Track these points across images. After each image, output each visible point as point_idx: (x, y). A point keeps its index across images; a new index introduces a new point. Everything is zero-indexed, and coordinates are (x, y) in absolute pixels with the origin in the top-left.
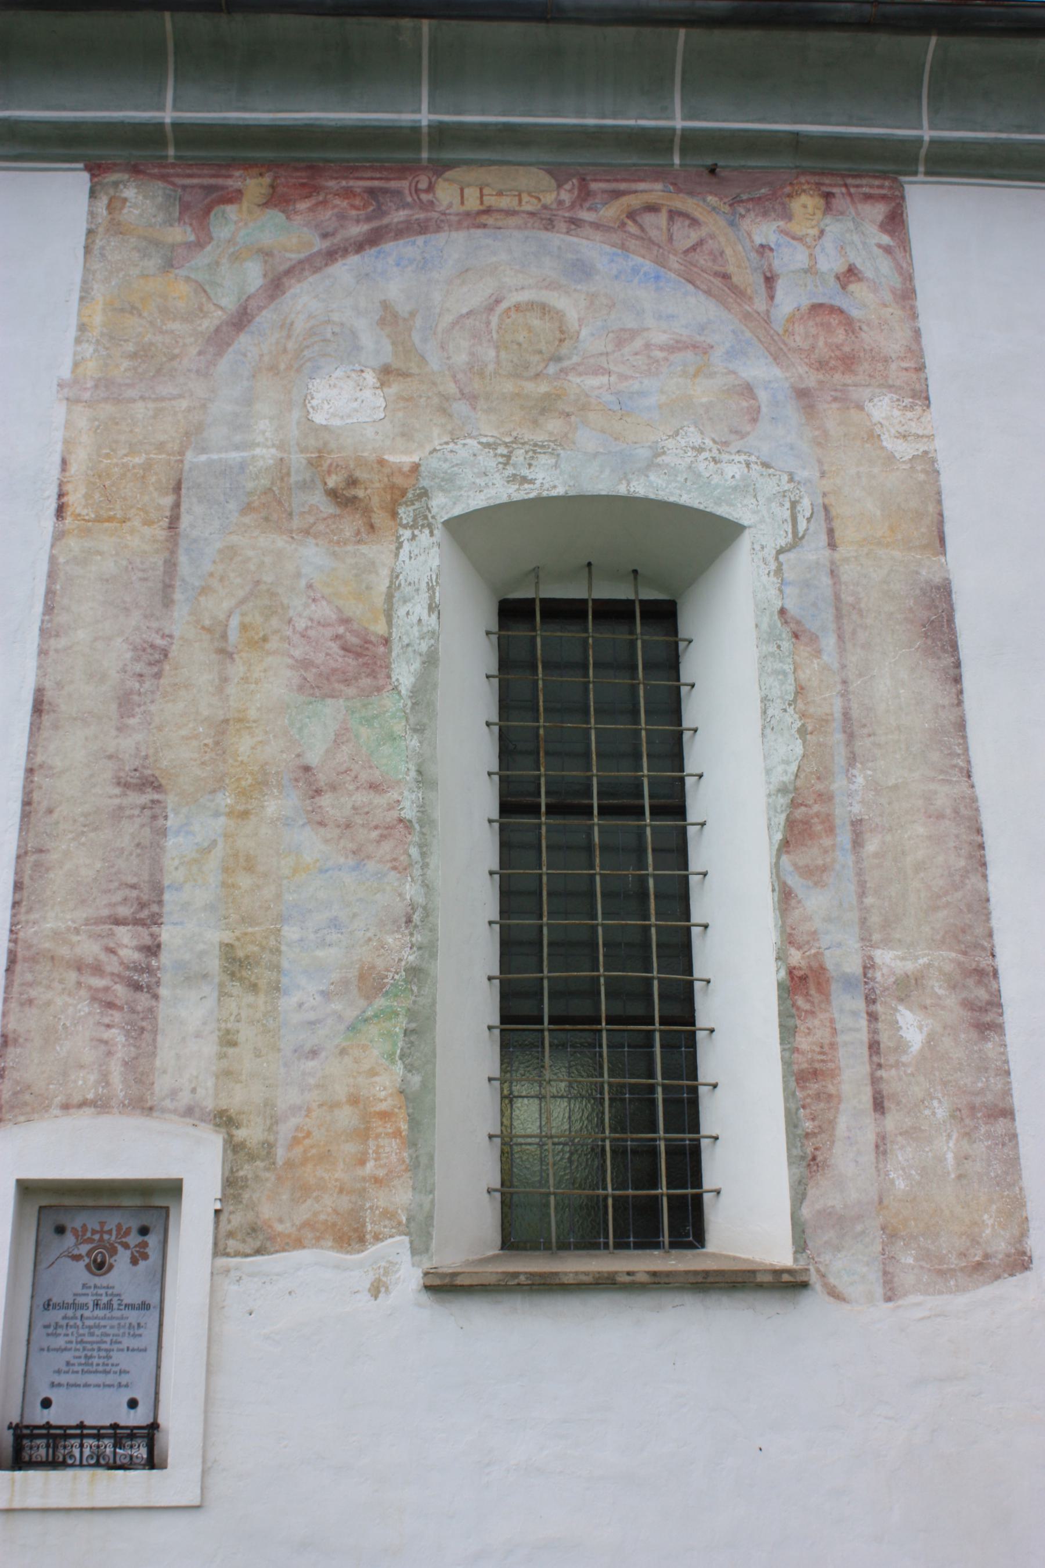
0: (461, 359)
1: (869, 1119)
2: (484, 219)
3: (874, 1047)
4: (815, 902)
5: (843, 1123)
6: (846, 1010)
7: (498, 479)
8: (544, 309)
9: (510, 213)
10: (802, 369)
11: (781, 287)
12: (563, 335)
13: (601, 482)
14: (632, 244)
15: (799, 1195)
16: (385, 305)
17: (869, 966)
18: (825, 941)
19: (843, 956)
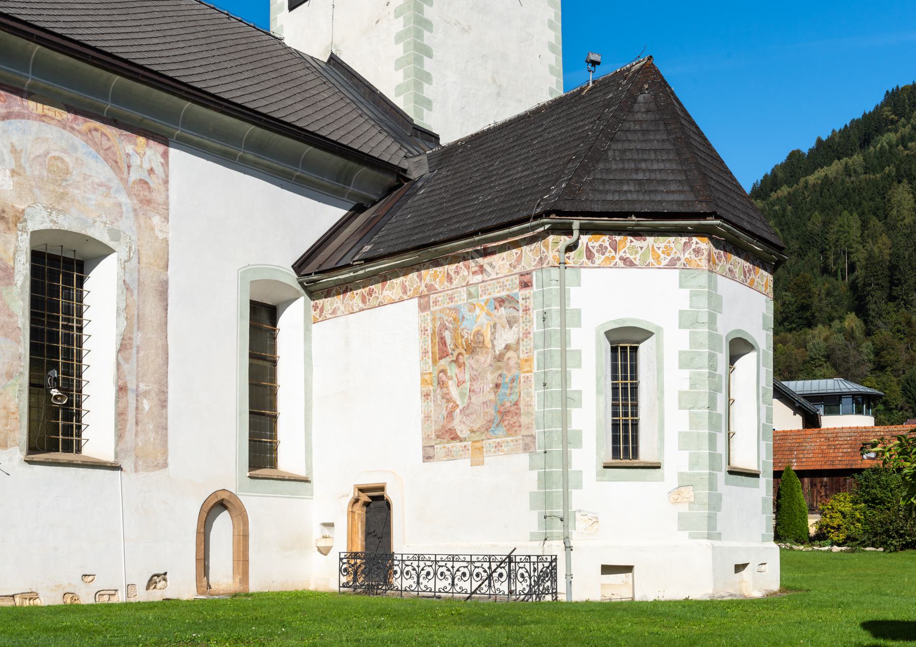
0: (37, 173)
1: (134, 426)
2: (43, 118)
3: (137, 408)
4: (125, 367)
5: (128, 426)
6: (131, 397)
7: (47, 220)
8: (62, 160)
9: (52, 119)
10: (135, 201)
11: (132, 169)
12: (67, 172)
13: (76, 228)
14: (90, 142)
15: (117, 445)
16: (12, 145)
17: (138, 386)
18: (128, 378)
19: (131, 386)
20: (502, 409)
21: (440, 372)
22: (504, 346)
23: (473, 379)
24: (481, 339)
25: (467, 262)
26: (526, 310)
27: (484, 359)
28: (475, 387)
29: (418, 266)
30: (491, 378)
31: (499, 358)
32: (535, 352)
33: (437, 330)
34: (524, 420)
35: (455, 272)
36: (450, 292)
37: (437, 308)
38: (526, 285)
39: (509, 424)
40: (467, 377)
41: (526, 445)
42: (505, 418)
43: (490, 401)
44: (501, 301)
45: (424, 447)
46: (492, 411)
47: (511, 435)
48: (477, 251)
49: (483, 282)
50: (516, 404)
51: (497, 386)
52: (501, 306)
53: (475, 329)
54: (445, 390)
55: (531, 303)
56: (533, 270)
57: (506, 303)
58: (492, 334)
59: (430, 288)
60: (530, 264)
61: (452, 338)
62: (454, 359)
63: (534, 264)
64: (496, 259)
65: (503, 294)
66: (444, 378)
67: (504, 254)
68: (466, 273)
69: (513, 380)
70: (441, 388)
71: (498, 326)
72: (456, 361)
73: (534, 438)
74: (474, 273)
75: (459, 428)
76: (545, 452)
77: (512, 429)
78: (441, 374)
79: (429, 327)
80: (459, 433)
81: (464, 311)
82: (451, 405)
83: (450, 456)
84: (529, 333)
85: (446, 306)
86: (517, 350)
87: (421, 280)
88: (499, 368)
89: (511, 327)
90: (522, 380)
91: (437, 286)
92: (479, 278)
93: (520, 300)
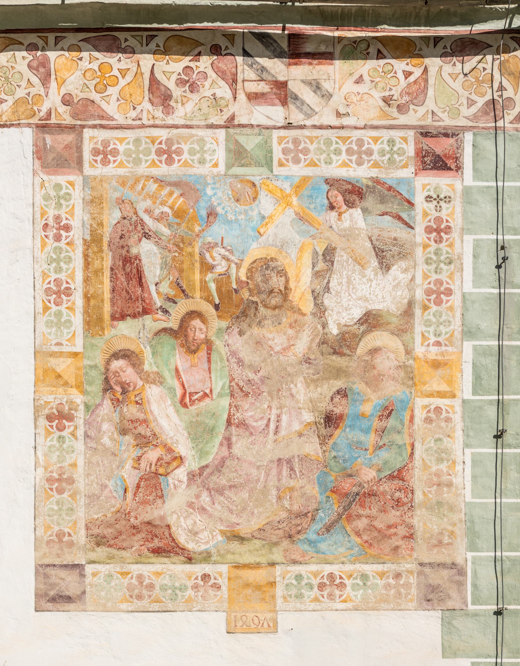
20: (347, 485)
21: (116, 356)
22: (357, 313)
23: (238, 391)
24: (276, 282)
25: (225, 63)
26: (439, 230)
27: (287, 341)
28: (250, 412)
29: (32, 38)
30: (306, 399)
31: (342, 344)
32: (468, 346)
33: (107, 233)
34: (421, 520)
35: (181, 82)
36: (163, 134)
37: (110, 170)
38: (439, 163)
39: (371, 527)
40: (219, 383)
41: (434, 589)
42: (356, 509)
43: (304, 459)
44: (353, 193)
45: (42, 570)
46: (309, 489)
47: (378, 559)
48: (263, 38)
49: (289, 126)
50: (398, 475)
51: (331, 420)
52: (350, 204)
53: (256, 251)
54: (131, 411)
55: (454, 214)
56: (465, 129)
57: (370, 201)
58: (317, 275)
59: (84, 111)
60: (455, 113)
61: (164, 265)
62: (173, 324)
63: (466, 112)
64: (336, 73)
65: (361, 173)
66: (129, 374)
67: (366, 67)
68: (224, 91)
69: (387, 411)
70: (117, 402)
71: (341, 257)
72: (180, 333)
73: (462, 572)
74: (254, 97)
75: (186, 523)
76: (498, 613)
77: (379, 543)
78: (117, 364)
79: (79, 220)
80: (182, 539)
81: (218, 196)
82: (153, 455)
83: (143, 597)
84: (449, 292)
85: (143, 169)
86: (403, 330)
87: (45, 80)
88: (339, 373)
89: (385, 266)
90: (420, 415)
91: (111, 108)
92: (276, 114)
93: (419, 200)
